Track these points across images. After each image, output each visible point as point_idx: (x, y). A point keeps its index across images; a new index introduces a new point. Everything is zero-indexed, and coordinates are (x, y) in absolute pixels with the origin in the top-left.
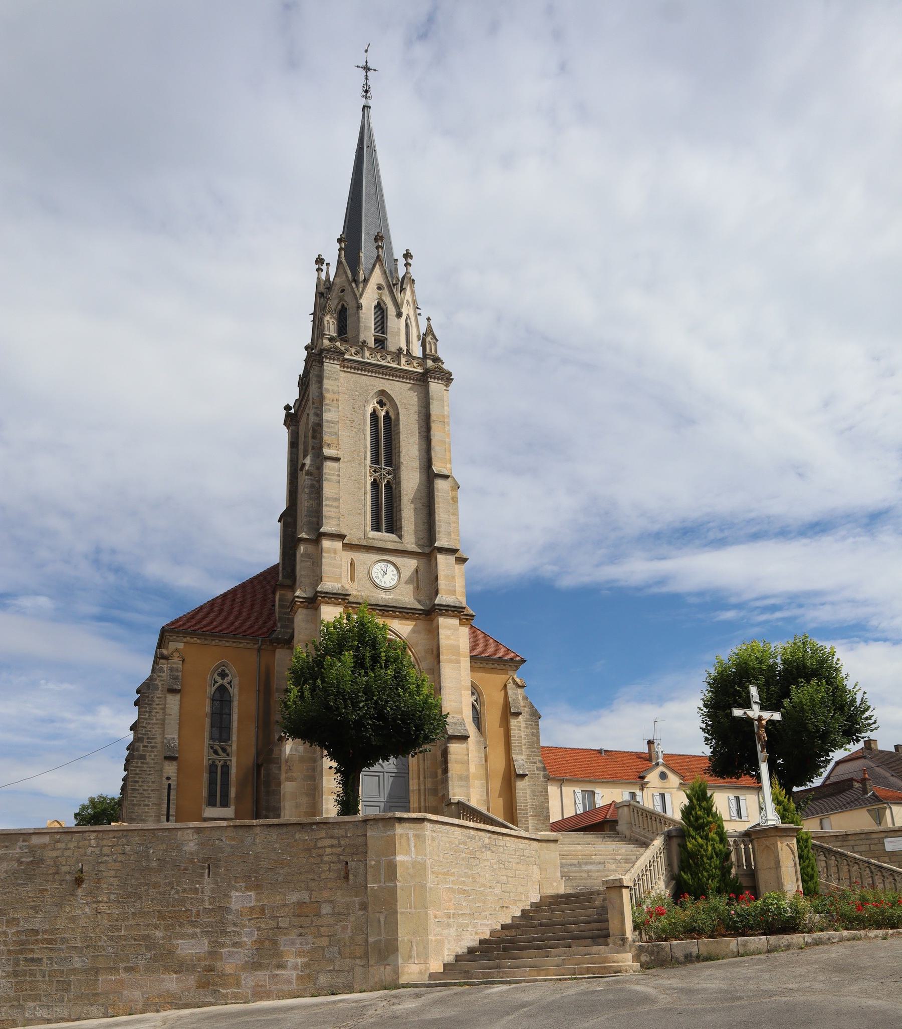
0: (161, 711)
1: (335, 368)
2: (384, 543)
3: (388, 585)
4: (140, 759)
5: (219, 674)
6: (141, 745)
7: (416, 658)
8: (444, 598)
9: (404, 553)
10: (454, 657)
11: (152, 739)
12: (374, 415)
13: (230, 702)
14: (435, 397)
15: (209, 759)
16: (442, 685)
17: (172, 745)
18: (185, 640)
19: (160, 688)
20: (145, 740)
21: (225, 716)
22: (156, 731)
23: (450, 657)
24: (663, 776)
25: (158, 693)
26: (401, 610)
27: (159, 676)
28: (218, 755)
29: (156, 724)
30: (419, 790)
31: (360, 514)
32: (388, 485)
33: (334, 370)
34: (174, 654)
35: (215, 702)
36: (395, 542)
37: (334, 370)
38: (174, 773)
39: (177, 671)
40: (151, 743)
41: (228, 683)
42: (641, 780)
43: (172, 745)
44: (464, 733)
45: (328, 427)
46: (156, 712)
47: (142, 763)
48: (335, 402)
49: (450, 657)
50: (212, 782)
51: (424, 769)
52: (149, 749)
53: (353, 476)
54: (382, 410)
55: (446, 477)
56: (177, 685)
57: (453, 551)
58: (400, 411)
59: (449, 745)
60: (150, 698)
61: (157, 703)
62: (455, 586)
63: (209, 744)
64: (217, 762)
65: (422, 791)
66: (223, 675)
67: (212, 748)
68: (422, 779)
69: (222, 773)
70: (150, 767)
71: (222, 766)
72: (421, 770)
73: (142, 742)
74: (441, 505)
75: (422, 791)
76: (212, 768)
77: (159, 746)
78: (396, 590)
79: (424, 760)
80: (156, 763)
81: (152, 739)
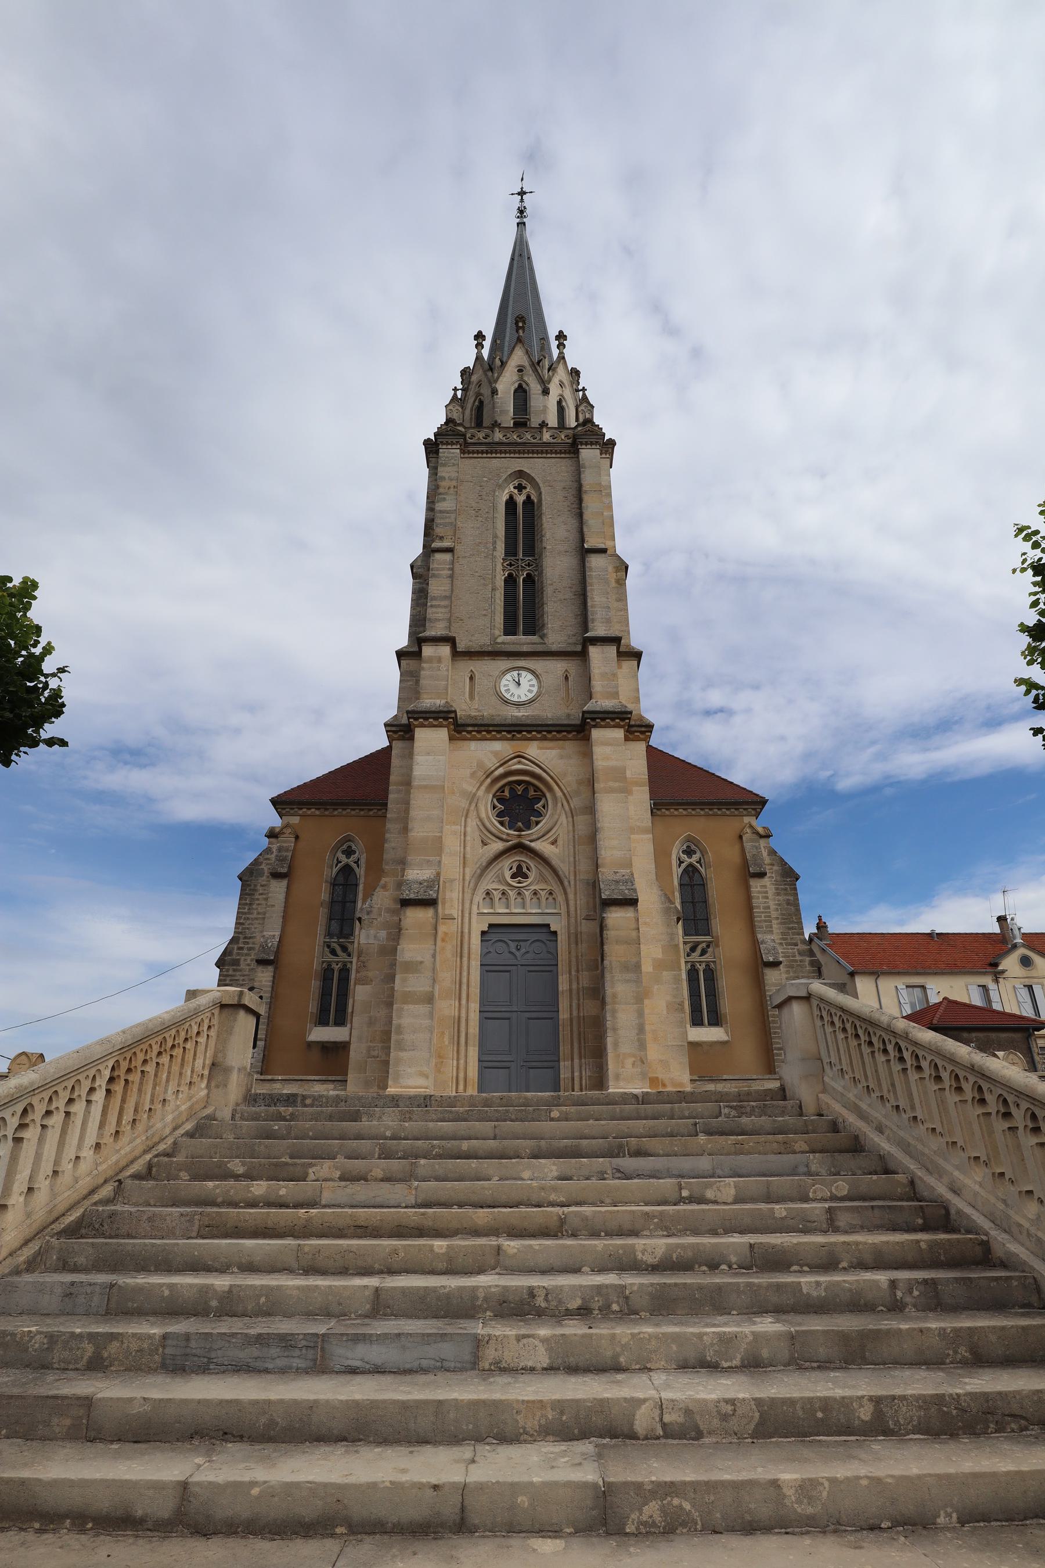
0: (263, 902)
1: (453, 453)
2: (518, 646)
3: (524, 699)
4: (233, 965)
5: (343, 852)
6: (236, 946)
7: (564, 794)
8: (599, 703)
9: (547, 656)
10: (617, 785)
11: (250, 938)
12: (511, 503)
13: (357, 885)
14: (587, 464)
15: (323, 962)
16: (599, 825)
17: (270, 945)
18: (300, 812)
19: (266, 874)
20: (241, 940)
21: (348, 904)
22: (255, 928)
23: (611, 784)
24: (1026, 962)
25: (263, 880)
26: (540, 728)
27: (266, 859)
28: (338, 956)
29: (256, 919)
30: (571, 990)
31: (485, 615)
32: (529, 580)
33: (451, 455)
34: (284, 830)
35: (337, 887)
36: (535, 644)
37: (451, 455)
38: (269, 981)
39: (287, 850)
40: (248, 943)
41: (355, 863)
42: (993, 968)
43: (270, 945)
44: (628, 894)
45: (441, 518)
46: (259, 904)
47: (234, 970)
48: (452, 489)
49: (611, 784)
50: (325, 994)
51: (577, 957)
52: (245, 951)
53: (477, 572)
54: (520, 495)
55: (604, 551)
56: (283, 867)
57: (616, 640)
58: (543, 490)
59: (605, 915)
60: (252, 887)
61: (261, 892)
62: (617, 687)
63: (325, 942)
64: (334, 966)
65: (574, 992)
66: (349, 852)
67: (329, 946)
68: (573, 973)
69: (339, 980)
70: (244, 976)
71: (341, 971)
72: (574, 959)
73: (238, 943)
74: (595, 587)
75: (574, 992)
76: (327, 974)
77: (257, 947)
78: (536, 705)
79: (577, 944)
80: (252, 969)
81: (250, 938)
